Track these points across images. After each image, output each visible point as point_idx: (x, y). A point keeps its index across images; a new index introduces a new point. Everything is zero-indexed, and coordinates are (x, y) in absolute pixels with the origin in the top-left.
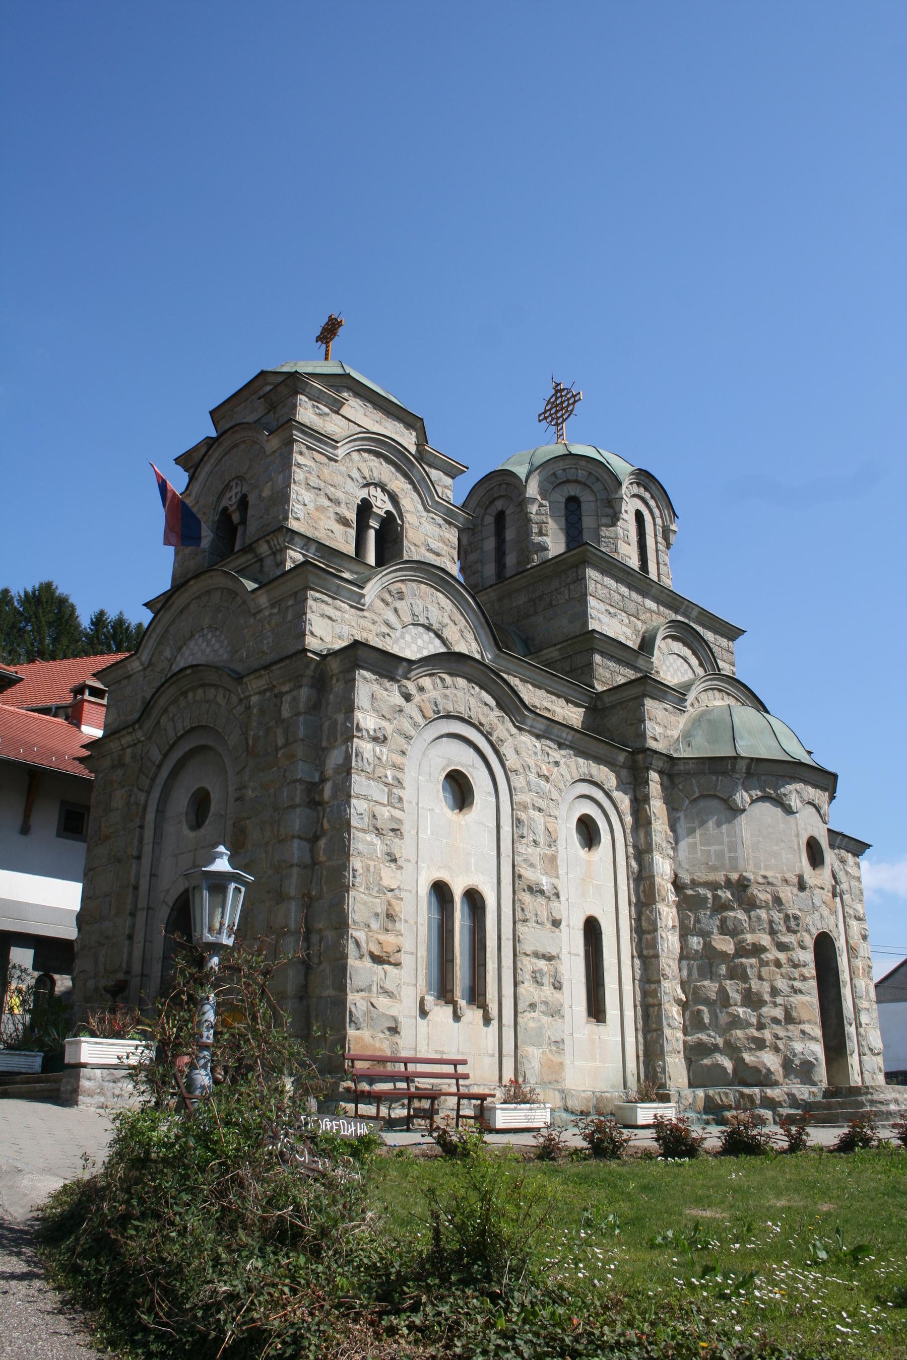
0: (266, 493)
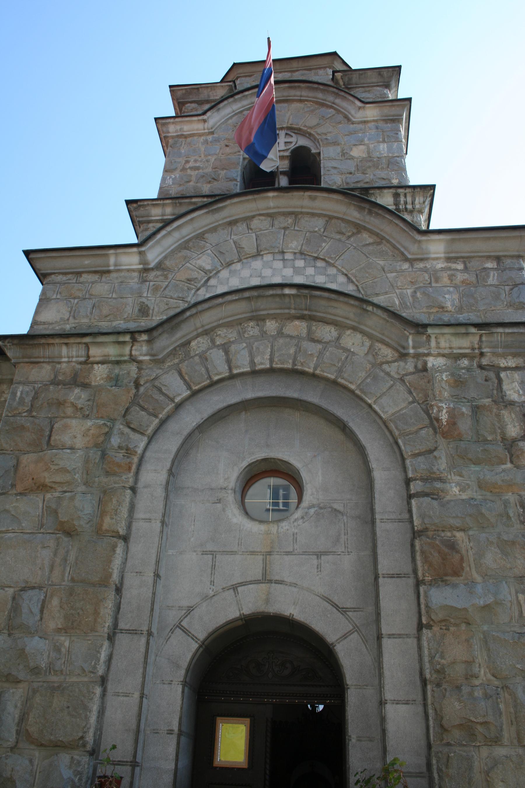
0: (358, 152)
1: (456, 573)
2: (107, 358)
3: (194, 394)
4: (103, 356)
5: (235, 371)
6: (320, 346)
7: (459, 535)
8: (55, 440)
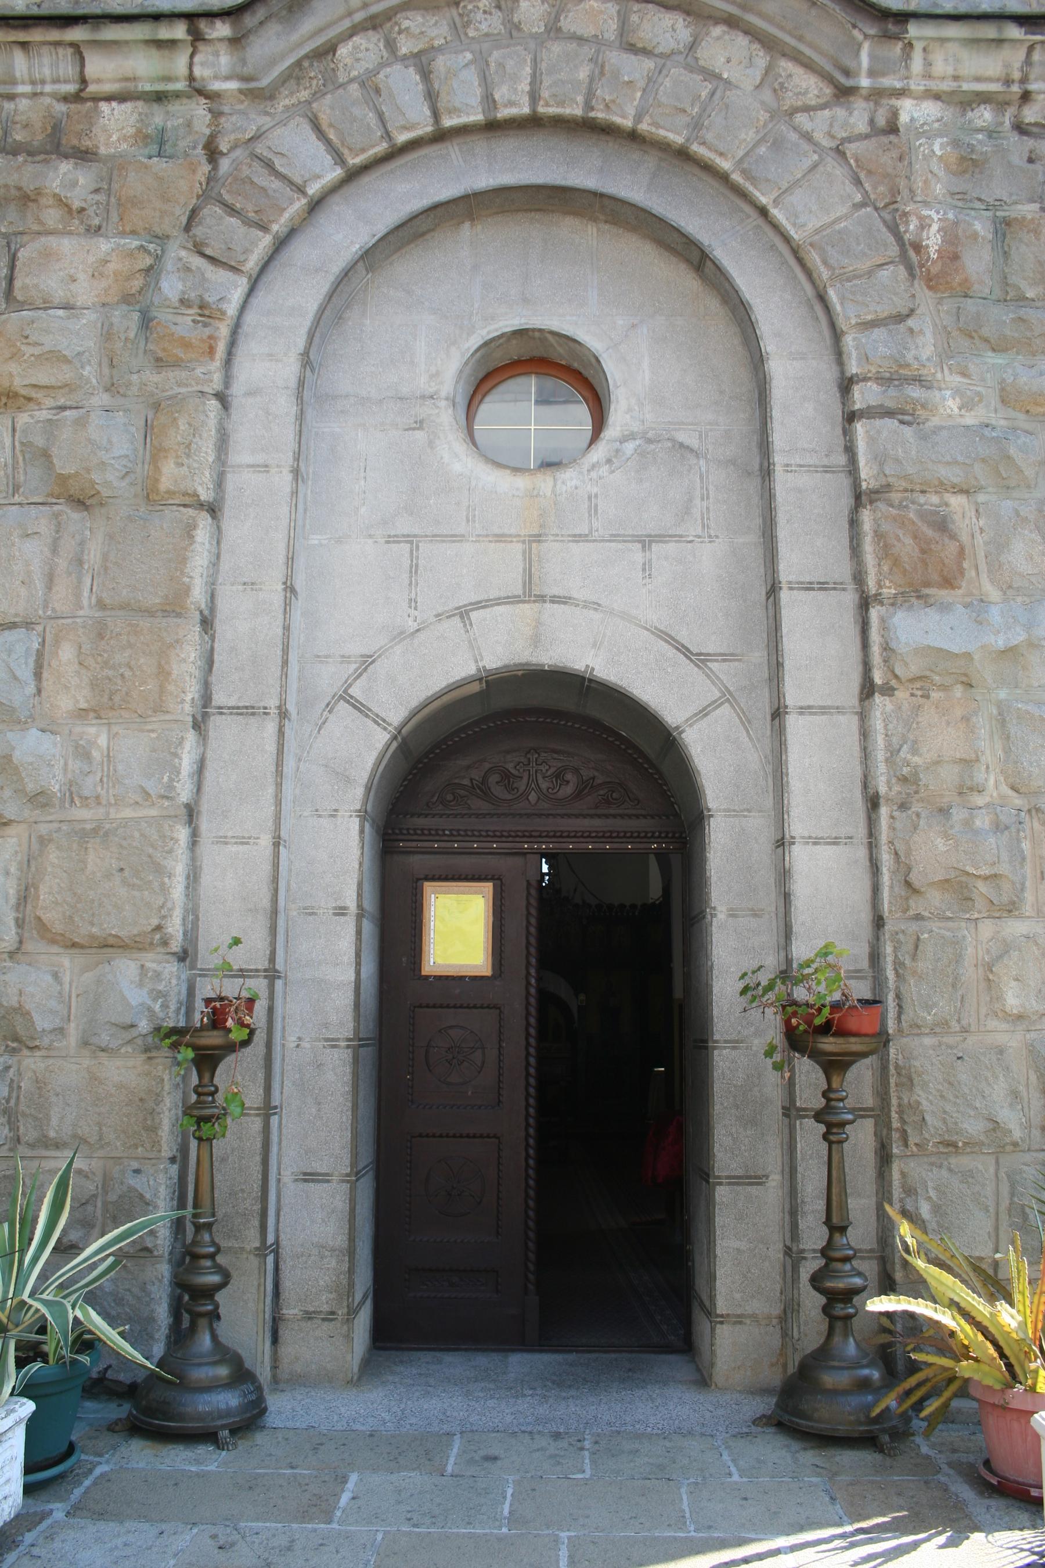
1: (948, 583)
2: (130, 86)
3: (353, 175)
4: (120, 80)
5: (448, 122)
6: (649, 64)
7: (957, 502)
8: (25, 287)
